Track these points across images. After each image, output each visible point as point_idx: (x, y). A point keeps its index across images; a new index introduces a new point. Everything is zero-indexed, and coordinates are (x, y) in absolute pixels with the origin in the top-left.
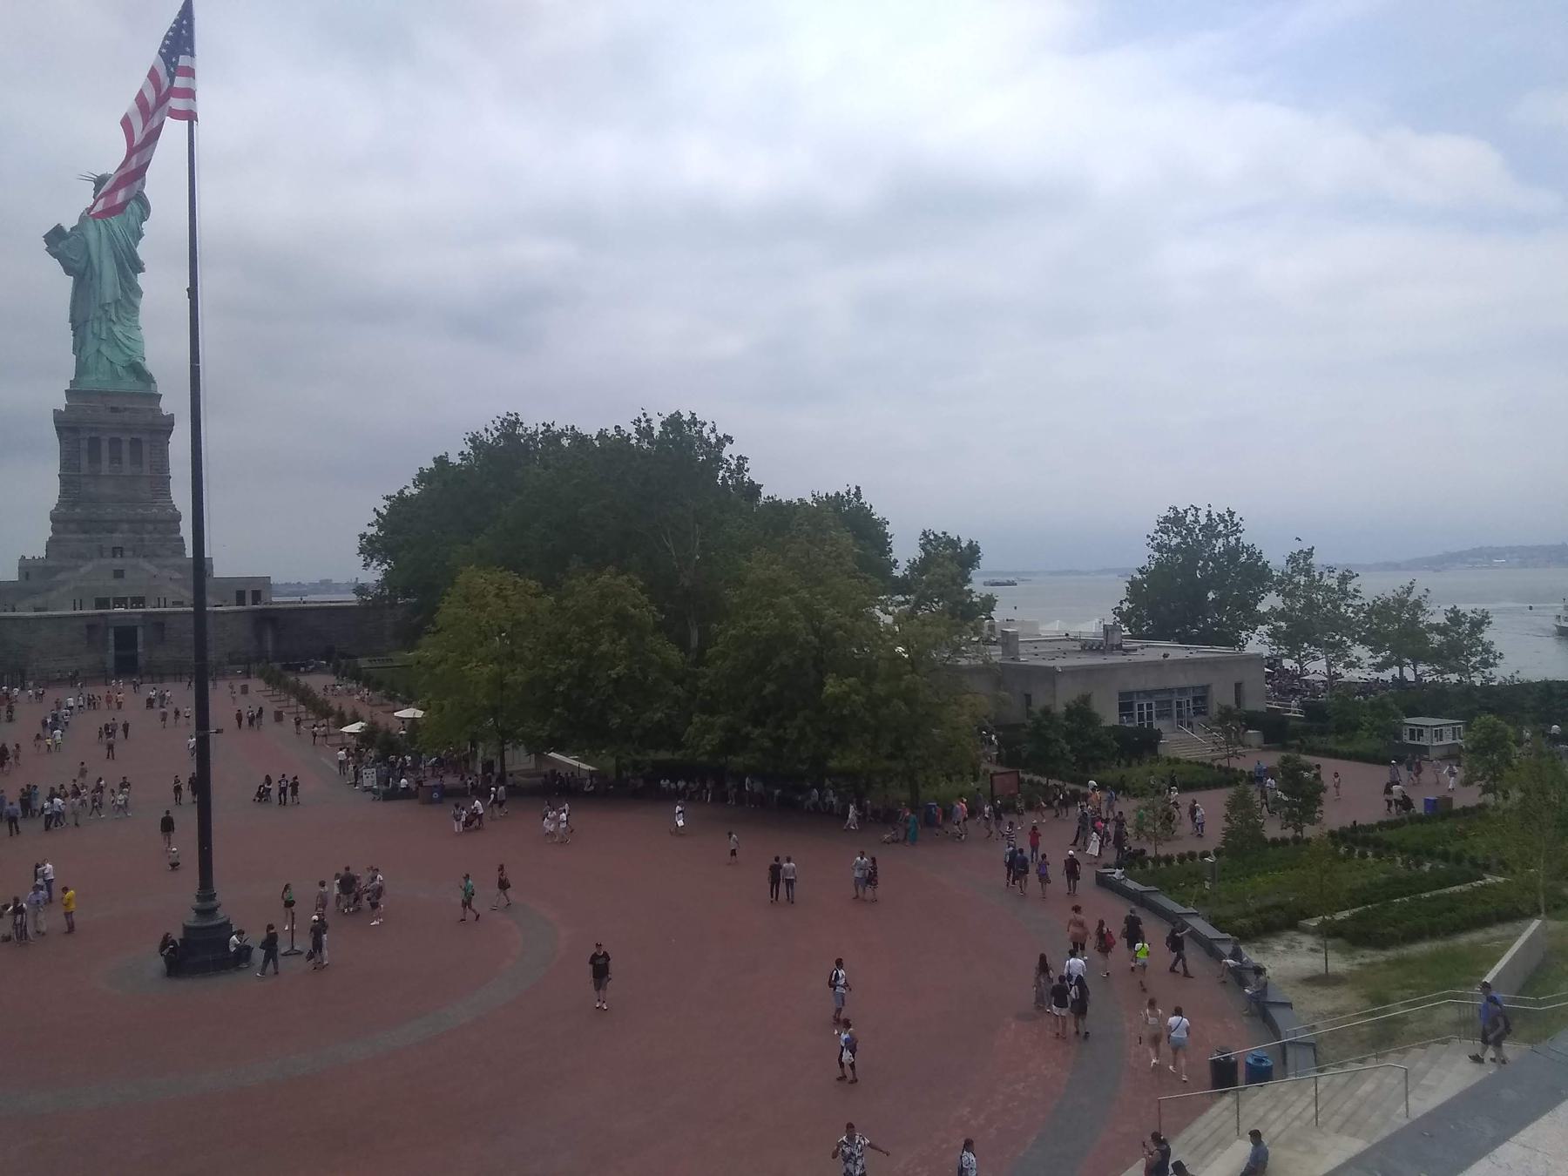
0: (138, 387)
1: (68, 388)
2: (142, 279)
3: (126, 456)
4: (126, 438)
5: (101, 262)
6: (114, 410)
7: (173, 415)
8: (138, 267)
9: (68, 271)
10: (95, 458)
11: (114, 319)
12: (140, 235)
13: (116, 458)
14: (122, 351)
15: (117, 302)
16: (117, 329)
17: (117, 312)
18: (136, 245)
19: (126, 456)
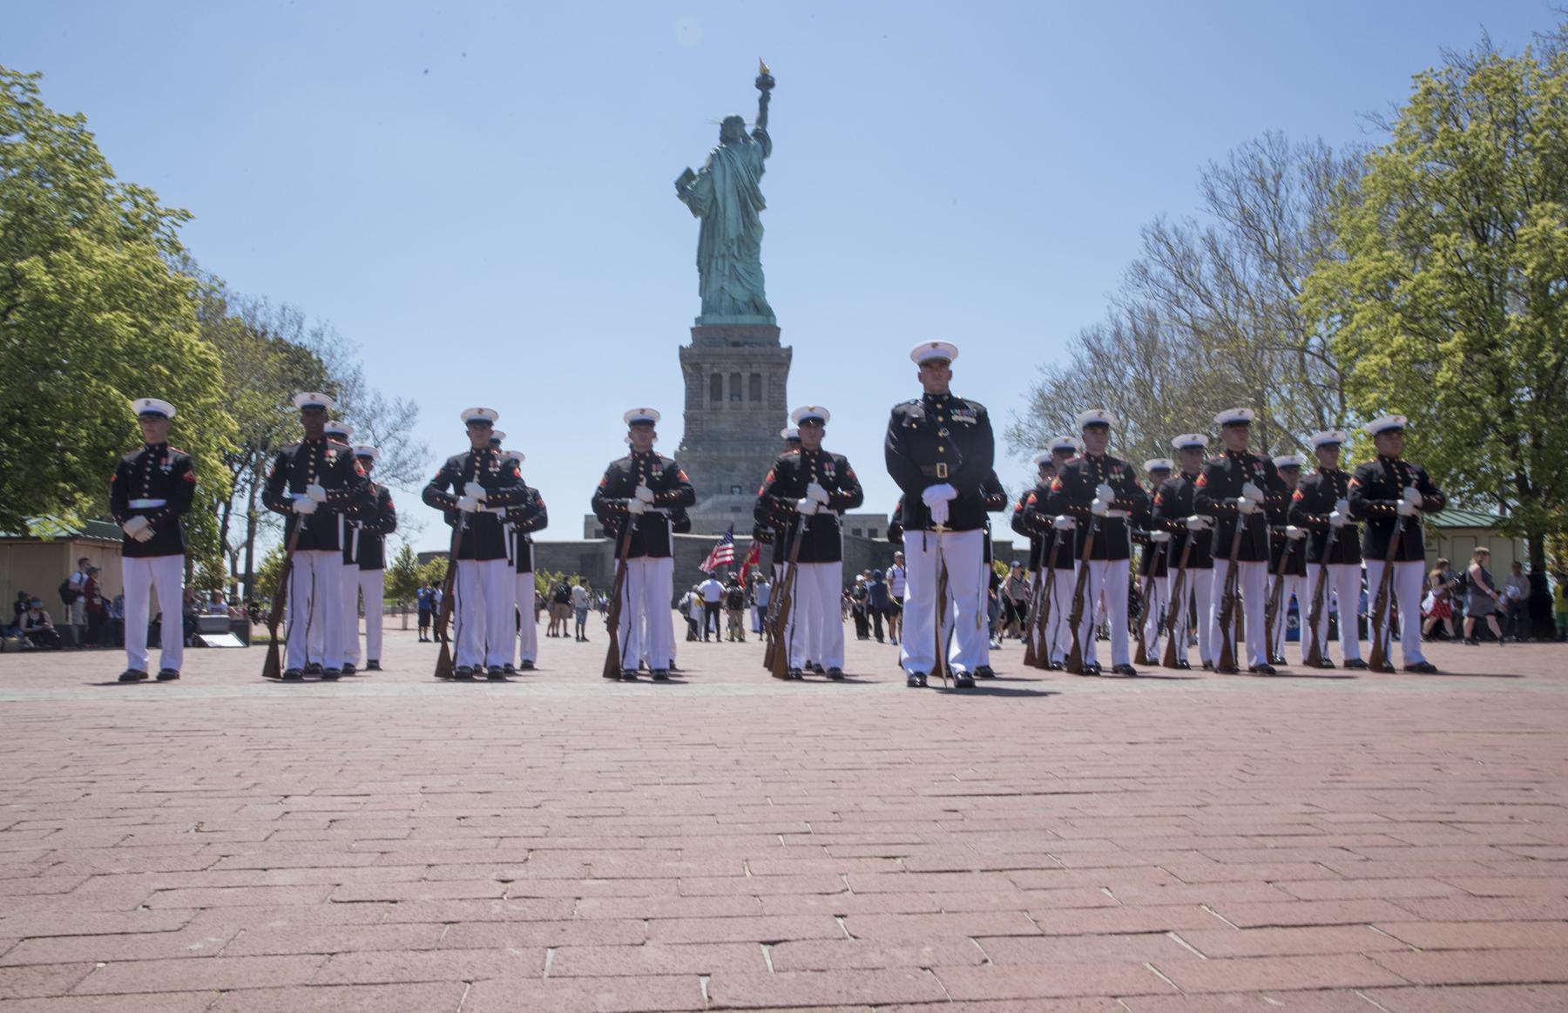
0: (758, 320)
1: (693, 325)
2: (763, 217)
3: (746, 393)
4: (746, 375)
5: (724, 198)
6: (735, 344)
7: (790, 348)
8: (760, 204)
9: (695, 211)
10: (716, 394)
11: (736, 254)
12: (762, 170)
13: (736, 395)
15: (740, 239)
16: (739, 266)
17: (739, 247)
18: (758, 181)
19: (746, 393)
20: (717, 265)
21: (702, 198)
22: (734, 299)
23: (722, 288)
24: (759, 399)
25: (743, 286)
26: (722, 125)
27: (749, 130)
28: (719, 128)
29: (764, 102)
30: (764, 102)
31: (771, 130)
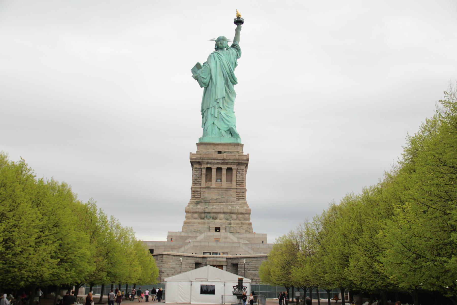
3: (224, 177)
8: (234, 82)
12: (236, 65)
14: (224, 122)
17: (223, 103)
19: (224, 177)
20: (211, 111)
21: (205, 77)
22: (219, 129)
23: (213, 123)
24: (231, 181)
25: (224, 122)
26: (216, 41)
27: (230, 44)
28: (215, 43)
29: (238, 31)
30: (238, 31)
31: (241, 44)
